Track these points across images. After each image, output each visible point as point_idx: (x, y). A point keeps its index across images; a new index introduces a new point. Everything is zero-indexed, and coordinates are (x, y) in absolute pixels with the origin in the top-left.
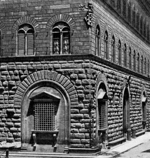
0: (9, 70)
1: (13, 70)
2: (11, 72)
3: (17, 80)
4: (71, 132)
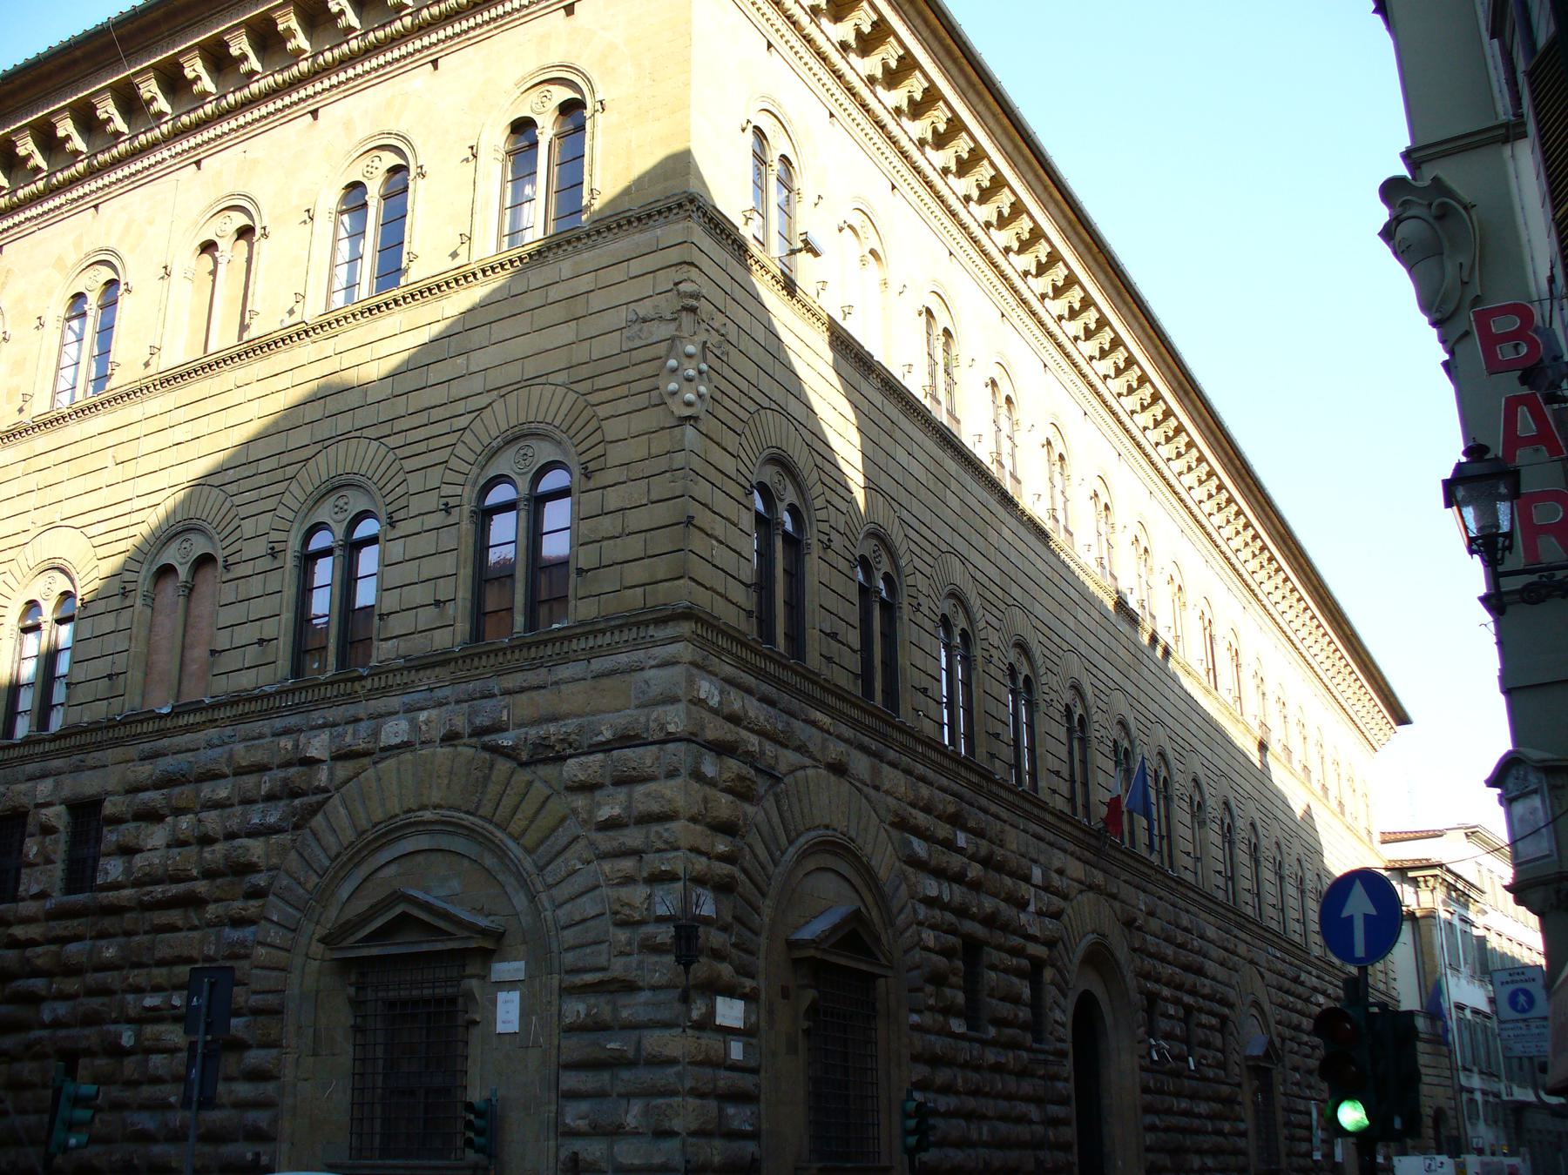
2: (249, 781)
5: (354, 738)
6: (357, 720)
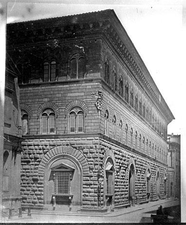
0: (34, 145)
1: (38, 145)
2: (36, 147)
3: (41, 154)
4: (83, 196)
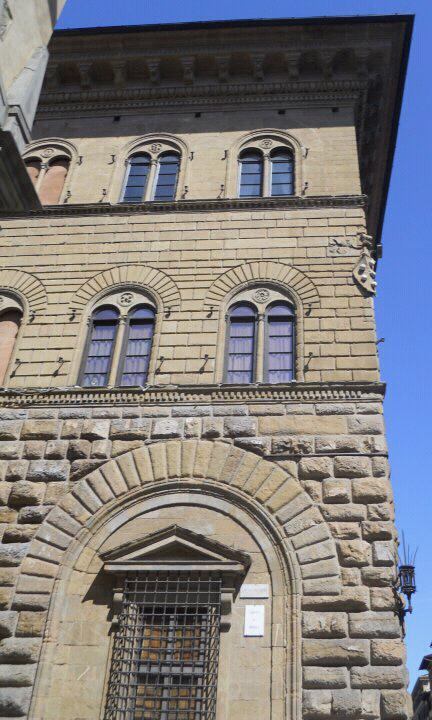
1: (47, 437)
2: (37, 446)
5: (126, 426)
6: (135, 417)
